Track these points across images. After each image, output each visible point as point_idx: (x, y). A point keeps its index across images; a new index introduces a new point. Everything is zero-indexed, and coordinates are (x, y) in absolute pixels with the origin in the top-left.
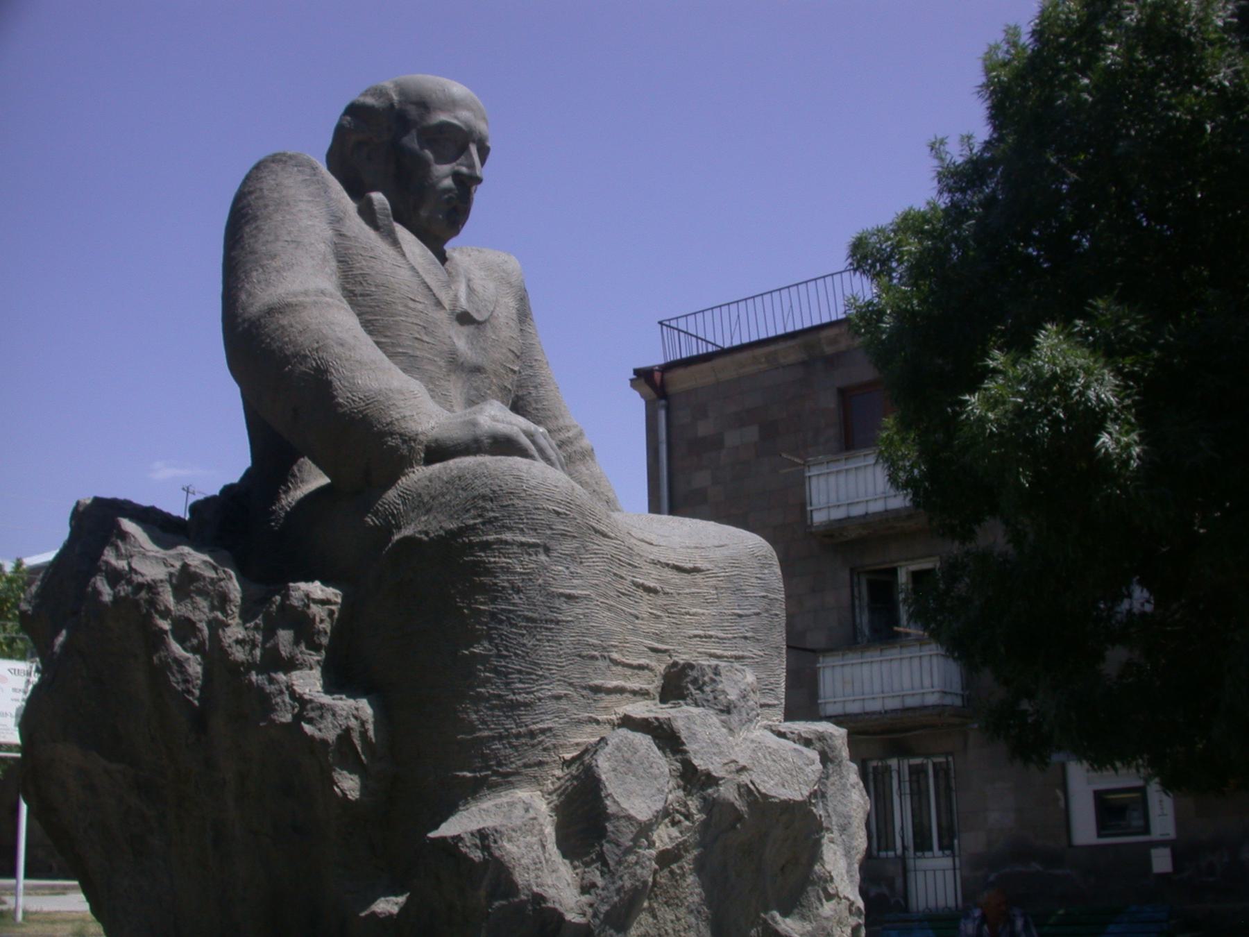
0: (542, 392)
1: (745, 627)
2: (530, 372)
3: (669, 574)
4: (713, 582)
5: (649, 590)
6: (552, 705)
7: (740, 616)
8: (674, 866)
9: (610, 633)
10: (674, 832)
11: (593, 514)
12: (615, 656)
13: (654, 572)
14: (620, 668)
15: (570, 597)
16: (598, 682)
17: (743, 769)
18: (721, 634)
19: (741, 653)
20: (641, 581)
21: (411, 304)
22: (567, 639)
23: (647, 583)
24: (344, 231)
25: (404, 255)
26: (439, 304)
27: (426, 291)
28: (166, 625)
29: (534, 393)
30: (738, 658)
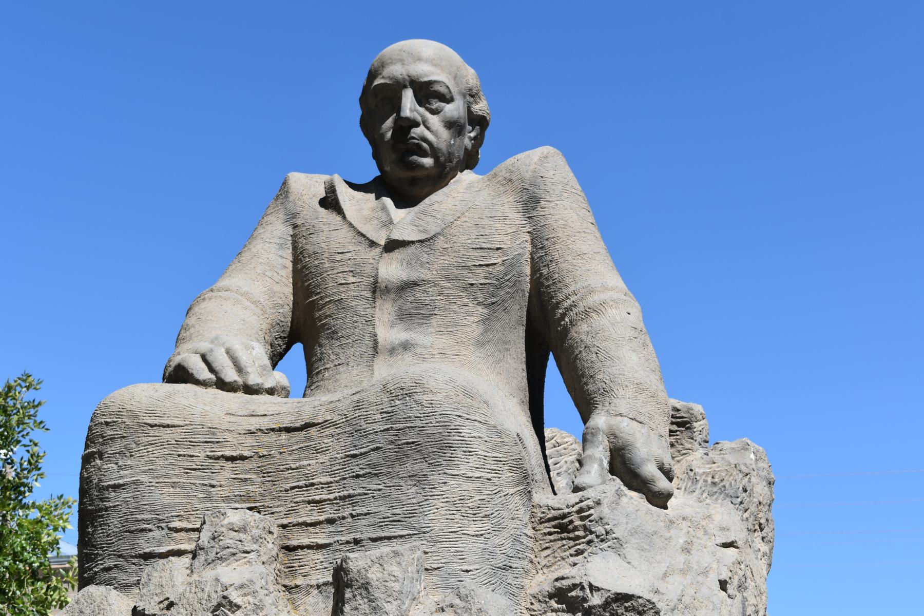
0: (553, 266)
2: (541, 253)
3: (273, 436)
5: (232, 459)
7: (354, 456)
11: (150, 413)
12: (177, 524)
13: (250, 441)
14: (183, 534)
15: (116, 487)
16: (147, 550)
18: (324, 479)
19: (346, 493)
20: (220, 454)
21: (339, 257)
23: (228, 453)
24: (299, 222)
25: (344, 217)
26: (373, 244)
27: (362, 239)
29: (545, 271)
30: (343, 498)
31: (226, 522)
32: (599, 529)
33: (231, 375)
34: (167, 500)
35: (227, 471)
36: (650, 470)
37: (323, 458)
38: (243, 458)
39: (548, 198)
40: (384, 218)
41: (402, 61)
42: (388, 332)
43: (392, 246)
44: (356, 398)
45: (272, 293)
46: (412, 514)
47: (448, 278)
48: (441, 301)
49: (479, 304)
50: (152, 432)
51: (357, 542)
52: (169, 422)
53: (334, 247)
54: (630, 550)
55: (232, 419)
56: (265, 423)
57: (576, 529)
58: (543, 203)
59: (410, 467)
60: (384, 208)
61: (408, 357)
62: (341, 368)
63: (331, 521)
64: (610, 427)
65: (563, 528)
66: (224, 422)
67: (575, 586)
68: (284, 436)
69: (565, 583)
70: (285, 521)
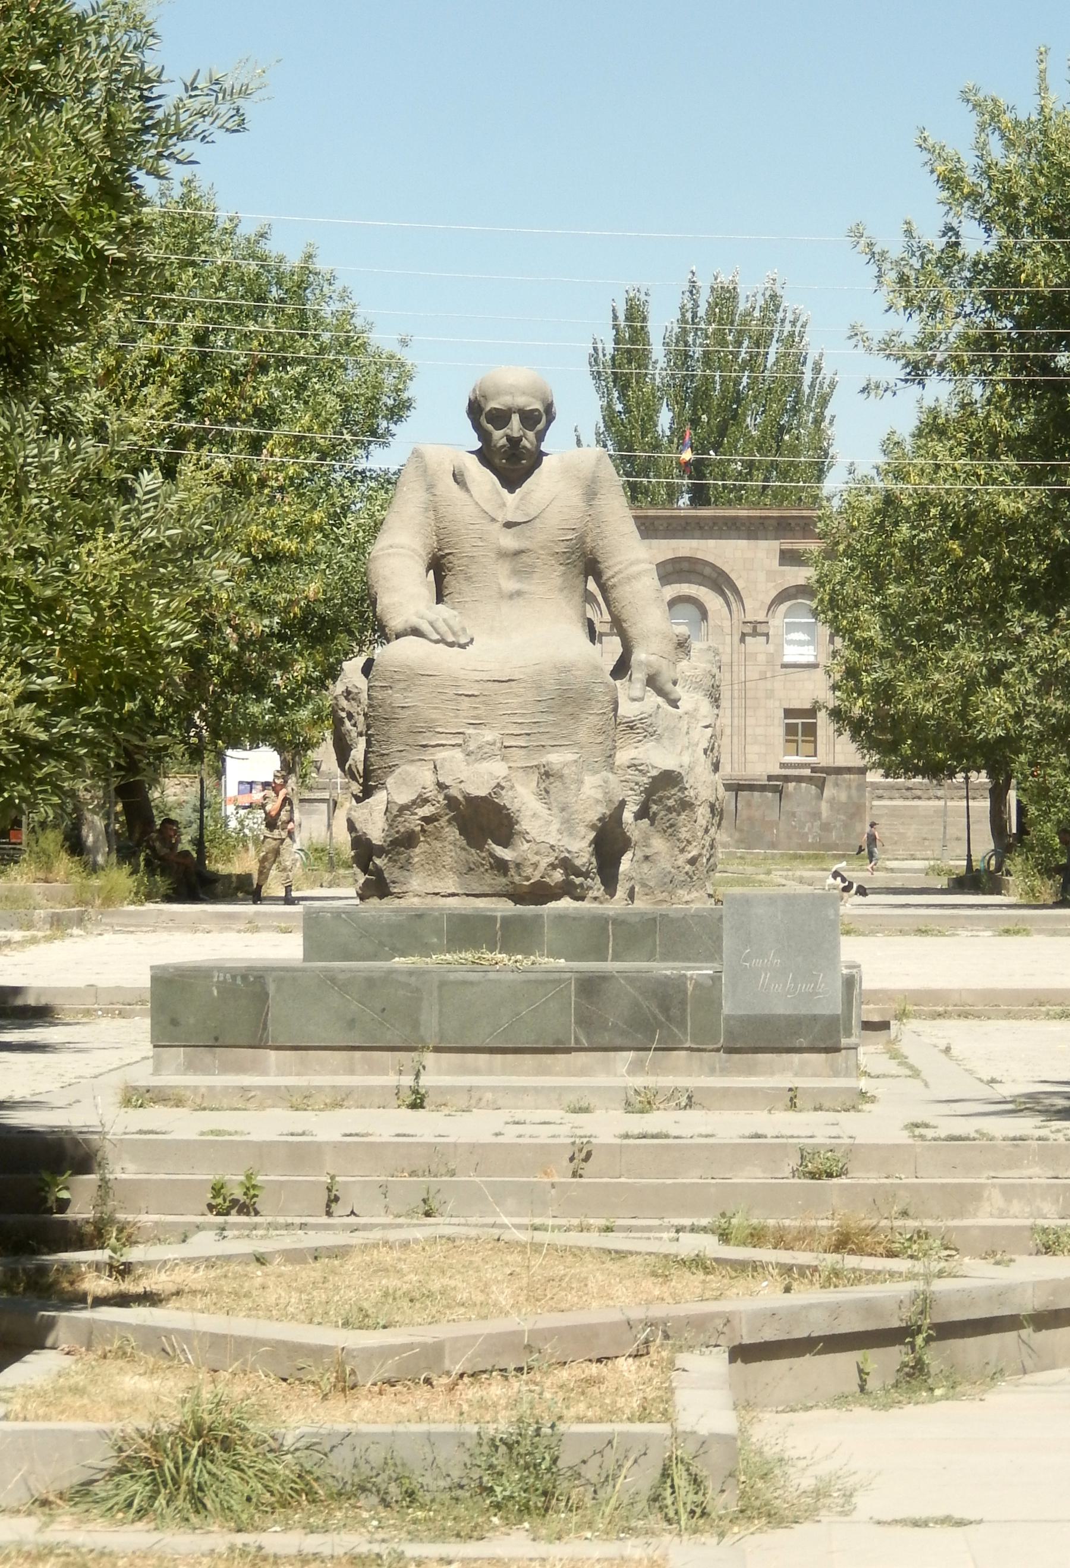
1: (541, 707)
9: (433, 720)
10: (432, 809)
13: (477, 686)
22: (403, 726)
26: (493, 520)
28: (344, 715)
32: (650, 730)
35: (466, 703)
36: (669, 686)
37: (520, 700)
42: (510, 585)
43: (509, 525)
47: (542, 548)
48: (539, 563)
54: (665, 741)
59: (569, 709)
60: (499, 493)
65: (632, 728)
69: (636, 762)
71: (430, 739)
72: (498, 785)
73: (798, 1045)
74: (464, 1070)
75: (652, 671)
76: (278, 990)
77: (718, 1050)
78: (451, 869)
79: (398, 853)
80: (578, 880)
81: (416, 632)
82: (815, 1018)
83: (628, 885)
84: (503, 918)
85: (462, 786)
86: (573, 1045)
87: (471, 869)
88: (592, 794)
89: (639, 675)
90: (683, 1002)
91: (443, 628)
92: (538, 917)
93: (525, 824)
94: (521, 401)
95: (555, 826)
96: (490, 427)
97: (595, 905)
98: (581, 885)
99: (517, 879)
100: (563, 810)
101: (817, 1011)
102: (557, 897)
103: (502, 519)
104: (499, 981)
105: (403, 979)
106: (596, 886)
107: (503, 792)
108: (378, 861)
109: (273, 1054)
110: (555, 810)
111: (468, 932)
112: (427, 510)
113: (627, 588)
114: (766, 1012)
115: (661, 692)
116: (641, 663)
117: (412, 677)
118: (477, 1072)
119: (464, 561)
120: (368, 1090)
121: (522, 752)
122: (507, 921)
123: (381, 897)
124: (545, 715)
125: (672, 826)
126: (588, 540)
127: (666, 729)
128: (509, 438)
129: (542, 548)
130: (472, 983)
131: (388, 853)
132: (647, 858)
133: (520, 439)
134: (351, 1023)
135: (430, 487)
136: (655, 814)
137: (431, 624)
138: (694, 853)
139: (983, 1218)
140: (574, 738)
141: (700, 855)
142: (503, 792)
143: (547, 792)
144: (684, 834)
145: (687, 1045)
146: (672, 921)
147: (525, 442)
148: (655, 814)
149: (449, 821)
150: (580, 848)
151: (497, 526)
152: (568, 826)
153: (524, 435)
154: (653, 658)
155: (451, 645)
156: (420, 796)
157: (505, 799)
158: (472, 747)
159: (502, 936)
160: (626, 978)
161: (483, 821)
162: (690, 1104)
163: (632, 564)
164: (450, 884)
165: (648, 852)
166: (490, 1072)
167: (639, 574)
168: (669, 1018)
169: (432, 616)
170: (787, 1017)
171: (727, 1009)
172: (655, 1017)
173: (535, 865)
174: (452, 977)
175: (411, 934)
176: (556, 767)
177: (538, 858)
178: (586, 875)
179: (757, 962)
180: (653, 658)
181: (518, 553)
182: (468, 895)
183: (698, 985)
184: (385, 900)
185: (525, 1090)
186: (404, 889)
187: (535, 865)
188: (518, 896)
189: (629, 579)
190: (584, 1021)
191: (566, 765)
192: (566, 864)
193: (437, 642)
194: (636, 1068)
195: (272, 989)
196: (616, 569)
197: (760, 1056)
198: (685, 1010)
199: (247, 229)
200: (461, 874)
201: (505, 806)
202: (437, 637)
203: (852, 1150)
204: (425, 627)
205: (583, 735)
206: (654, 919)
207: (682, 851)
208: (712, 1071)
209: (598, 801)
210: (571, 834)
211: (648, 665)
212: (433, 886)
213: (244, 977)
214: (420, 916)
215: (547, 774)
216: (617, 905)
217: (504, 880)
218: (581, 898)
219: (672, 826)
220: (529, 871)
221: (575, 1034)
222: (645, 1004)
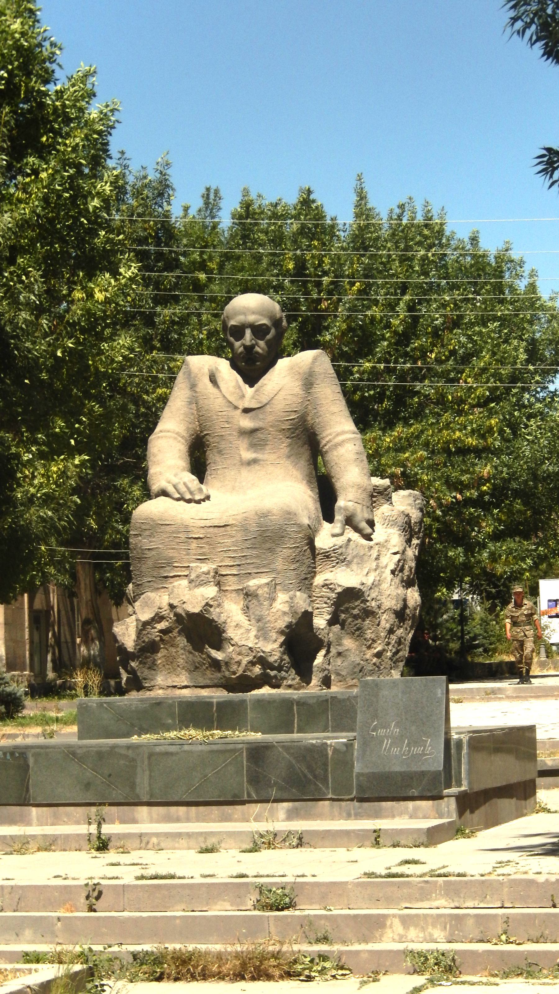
3: (211, 530)
4: (235, 528)
6: (148, 584)
8: (170, 634)
9: (172, 558)
10: (167, 623)
11: (161, 519)
13: (202, 531)
16: (165, 575)
17: (184, 602)
21: (220, 414)
22: (150, 563)
23: (194, 536)
25: (221, 391)
26: (236, 408)
29: (317, 420)
31: (201, 571)
33: (188, 496)
34: (171, 555)
35: (194, 545)
37: (234, 540)
38: (201, 538)
39: (317, 383)
40: (240, 394)
41: (245, 314)
42: (248, 455)
43: (246, 411)
44: (244, 515)
45: (188, 429)
46: (270, 564)
47: (271, 426)
49: (287, 438)
50: (163, 527)
51: (250, 574)
52: (168, 523)
53: (218, 408)
54: (354, 566)
55: (192, 521)
56: (208, 523)
57: (332, 557)
58: (315, 386)
59: (268, 545)
60: (239, 387)
61: (257, 467)
62: (226, 471)
63: (239, 565)
64: (346, 506)
65: (328, 557)
66: (191, 523)
67: (332, 584)
68: (216, 530)
70: (220, 564)
71: (169, 572)
72: (207, 604)
73: (411, 795)
74: (168, 819)
75: (349, 514)
76: (36, 761)
77: (352, 800)
78: (183, 668)
79: (146, 658)
80: (273, 673)
81: (164, 493)
82: (423, 773)
83: (321, 675)
84: (218, 704)
85: (184, 606)
86: (246, 798)
87: (197, 668)
88: (282, 607)
89: (339, 517)
90: (326, 764)
91: (183, 489)
92: (243, 702)
93: (230, 633)
94: (251, 318)
95: (253, 633)
96: (232, 339)
97: (290, 691)
98: (275, 677)
99: (227, 674)
100: (259, 621)
101: (424, 768)
102: (260, 687)
103: (241, 407)
104: (191, 752)
105: (123, 752)
106: (293, 678)
107: (212, 610)
108: (133, 664)
109: (34, 810)
110: (253, 621)
111: (195, 714)
112: (190, 403)
113: (335, 453)
114: (387, 769)
115: (357, 529)
116: (340, 508)
117: (155, 526)
118: (178, 820)
119: (216, 439)
120: (67, 837)
121: (235, 578)
122: (222, 706)
123: (138, 691)
124: (250, 550)
125: (358, 629)
126: (309, 418)
127: (354, 557)
128: (245, 347)
129: (271, 426)
130: (172, 754)
131: (138, 657)
132: (339, 654)
133: (252, 347)
134: (88, 786)
135: (193, 387)
136: (344, 621)
137: (175, 486)
138: (379, 648)
139: (387, 944)
140: (272, 566)
141: (384, 650)
142: (212, 610)
143: (248, 608)
144: (369, 634)
145: (329, 796)
146: (340, 701)
147: (257, 349)
148: (344, 621)
149: (179, 632)
150: (272, 648)
151: (239, 412)
152: (263, 633)
153: (257, 344)
154: (350, 504)
155: (189, 501)
156: (157, 614)
157: (214, 614)
158: (193, 576)
159: (218, 716)
160: (283, 747)
161: (202, 631)
162: (300, 844)
163: (338, 435)
164: (183, 679)
165: (340, 649)
166: (188, 820)
167: (343, 441)
168: (315, 777)
169: (175, 480)
170: (401, 773)
171: (358, 768)
172: (305, 776)
173: (239, 663)
174: (158, 749)
175: (154, 717)
176: (252, 589)
177: (240, 657)
178: (280, 669)
179: (381, 732)
180: (350, 504)
181: (253, 431)
182: (196, 687)
183: (336, 751)
184: (141, 693)
185: (179, 835)
186: (152, 683)
187: (239, 663)
188: (231, 686)
189: (337, 446)
190: (256, 780)
191: (259, 587)
192: (262, 661)
193: (178, 500)
194: (291, 816)
195: (31, 761)
196: (327, 439)
197: (384, 804)
198: (326, 770)
199: (463, 235)
200: (190, 671)
201: (213, 620)
202: (177, 496)
203: (295, 886)
204: (170, 489)
205: (279, 564)
206: (327, 701)
207: (369, 647)
208: (349, 816)
209: (285, 613)
210: (265, 639)
211: (346, 509)
212: (172, 682)
213: (12, 754)
214: (158, 703)
215: (247, 595)
216: (314, 688)
217: (219, 675)
218: (278, 687)
219: (358, 629)
220: (234, 667)
221: (247, 789)
222: (297, 766)
